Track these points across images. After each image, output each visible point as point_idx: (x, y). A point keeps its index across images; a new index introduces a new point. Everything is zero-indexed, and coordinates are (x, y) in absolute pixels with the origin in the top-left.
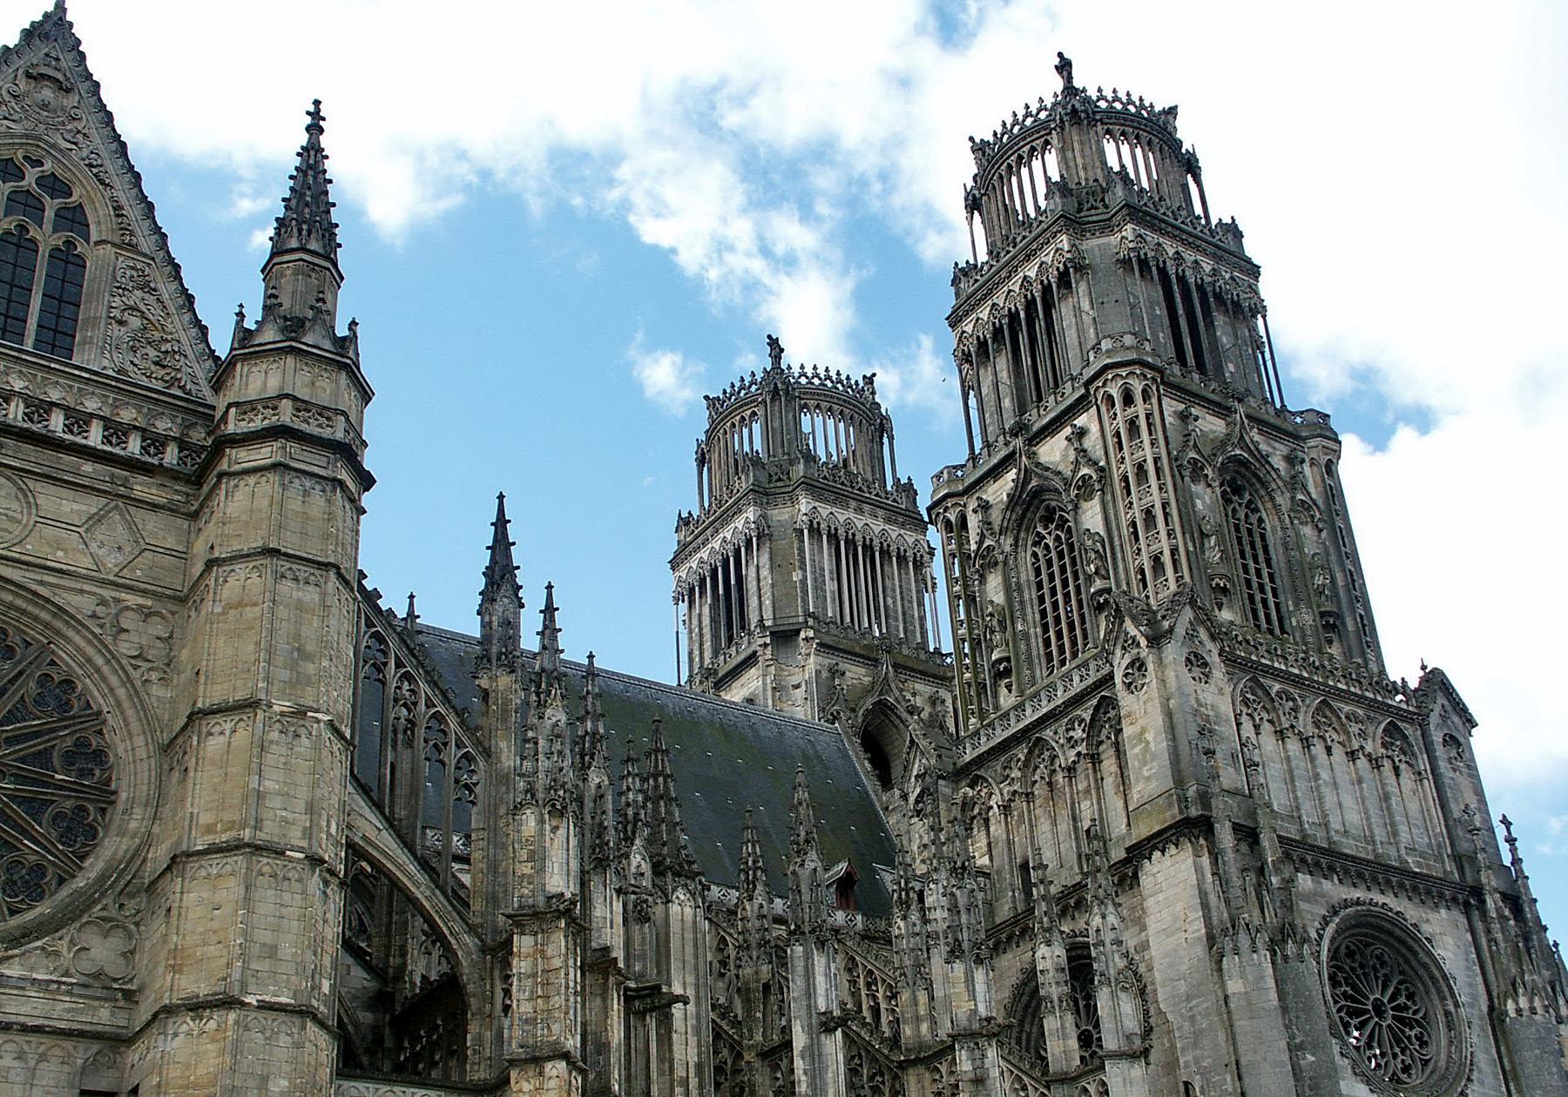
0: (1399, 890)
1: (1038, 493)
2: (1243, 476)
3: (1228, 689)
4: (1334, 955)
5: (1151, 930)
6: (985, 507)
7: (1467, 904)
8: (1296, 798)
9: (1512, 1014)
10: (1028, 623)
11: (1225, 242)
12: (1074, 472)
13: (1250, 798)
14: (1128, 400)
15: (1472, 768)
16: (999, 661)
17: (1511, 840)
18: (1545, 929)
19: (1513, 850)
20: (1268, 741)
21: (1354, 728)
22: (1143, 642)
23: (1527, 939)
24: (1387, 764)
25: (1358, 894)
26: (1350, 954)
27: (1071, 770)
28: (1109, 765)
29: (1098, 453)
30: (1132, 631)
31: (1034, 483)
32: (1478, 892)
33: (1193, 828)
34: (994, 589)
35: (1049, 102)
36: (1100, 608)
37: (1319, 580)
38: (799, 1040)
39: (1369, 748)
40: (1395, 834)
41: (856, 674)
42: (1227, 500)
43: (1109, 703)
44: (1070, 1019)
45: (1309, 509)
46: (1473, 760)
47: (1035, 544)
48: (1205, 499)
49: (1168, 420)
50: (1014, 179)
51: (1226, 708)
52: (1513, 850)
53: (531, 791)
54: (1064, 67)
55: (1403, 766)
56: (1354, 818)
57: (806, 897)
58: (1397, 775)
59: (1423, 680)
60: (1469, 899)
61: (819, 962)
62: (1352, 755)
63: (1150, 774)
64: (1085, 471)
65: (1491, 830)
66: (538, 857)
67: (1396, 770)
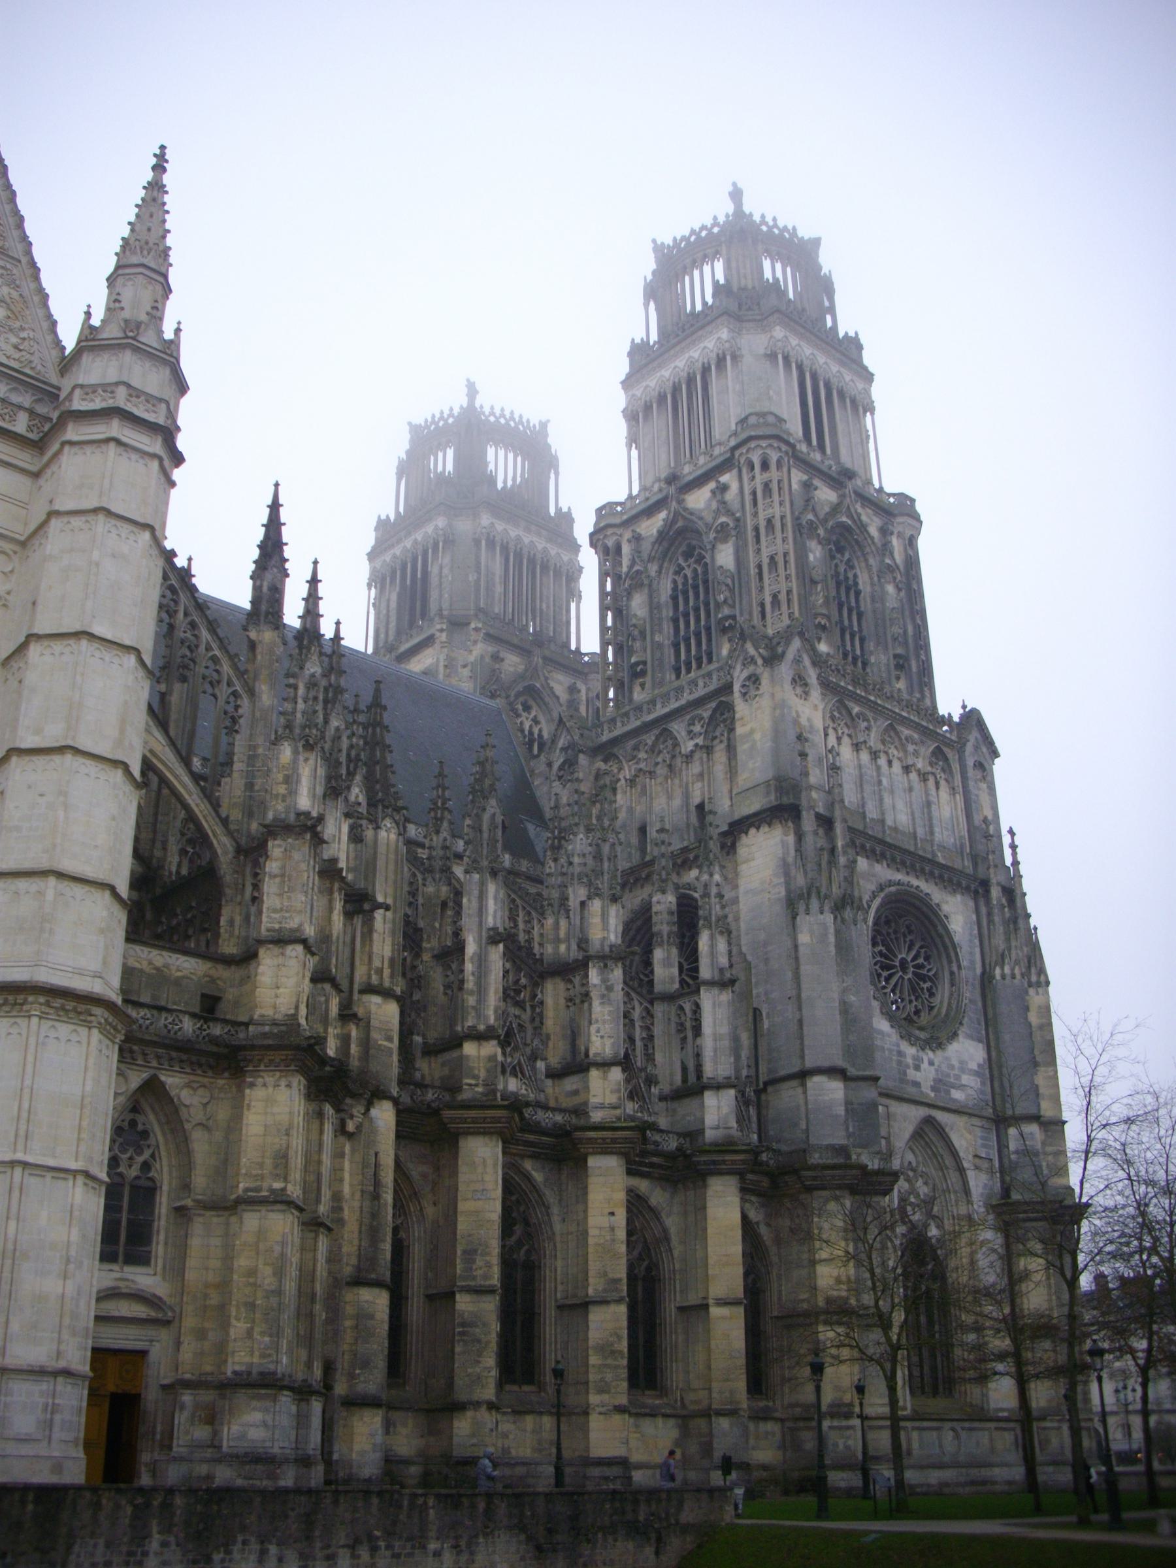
0: (930, 876)
1: (681, 532)
3: (821, 707)
4: (876, 923)
5: (742, 889)
6: (637, 539)
7: (976, 892)
9: (998, 977)
10: (664, 636)
11: (849, 351)
12: (715, 519)
13: (832, 793)
14: (765, 466)
16: (637, 664)
17: (1013, 847)
18: (1029, 916)
19: (1014, 854)
21: (911, 748)
22: (760, 661)
23: (1015, 922)
25: (899, 876)
26: (888, 922)
27: (689, 757)
28: (720, 755)
29: (736, 506)
30: (751, 651)
31: (680, 524)
32: (985, 884)
33: (783, 809)
34: (638, 605)
36: (724, 630)
37: (896, 630)
38: (471, 948)
39: (919, 765)
40: (932, 833)
41: (512, 663)
42: (833, 557)
43: (729, 707)
44: (674, 951)
45: (892, 571)
47: (677, 573)
48: (815, 553)
49: (795, 486)
50: (687, 278)
51: (819, 724)
52: (1014, 854)
53: (289, 726)
55: (943, 783)
56: (903, 819)
57: (485, 835)
58: (938, 788)
59: (962, 717)
60: (978, 889)
61: (491, 888)
62: (907, 769)
63: (755, 767)
64: (723, 519)
65: (1000, 837)
66: (291, 780)
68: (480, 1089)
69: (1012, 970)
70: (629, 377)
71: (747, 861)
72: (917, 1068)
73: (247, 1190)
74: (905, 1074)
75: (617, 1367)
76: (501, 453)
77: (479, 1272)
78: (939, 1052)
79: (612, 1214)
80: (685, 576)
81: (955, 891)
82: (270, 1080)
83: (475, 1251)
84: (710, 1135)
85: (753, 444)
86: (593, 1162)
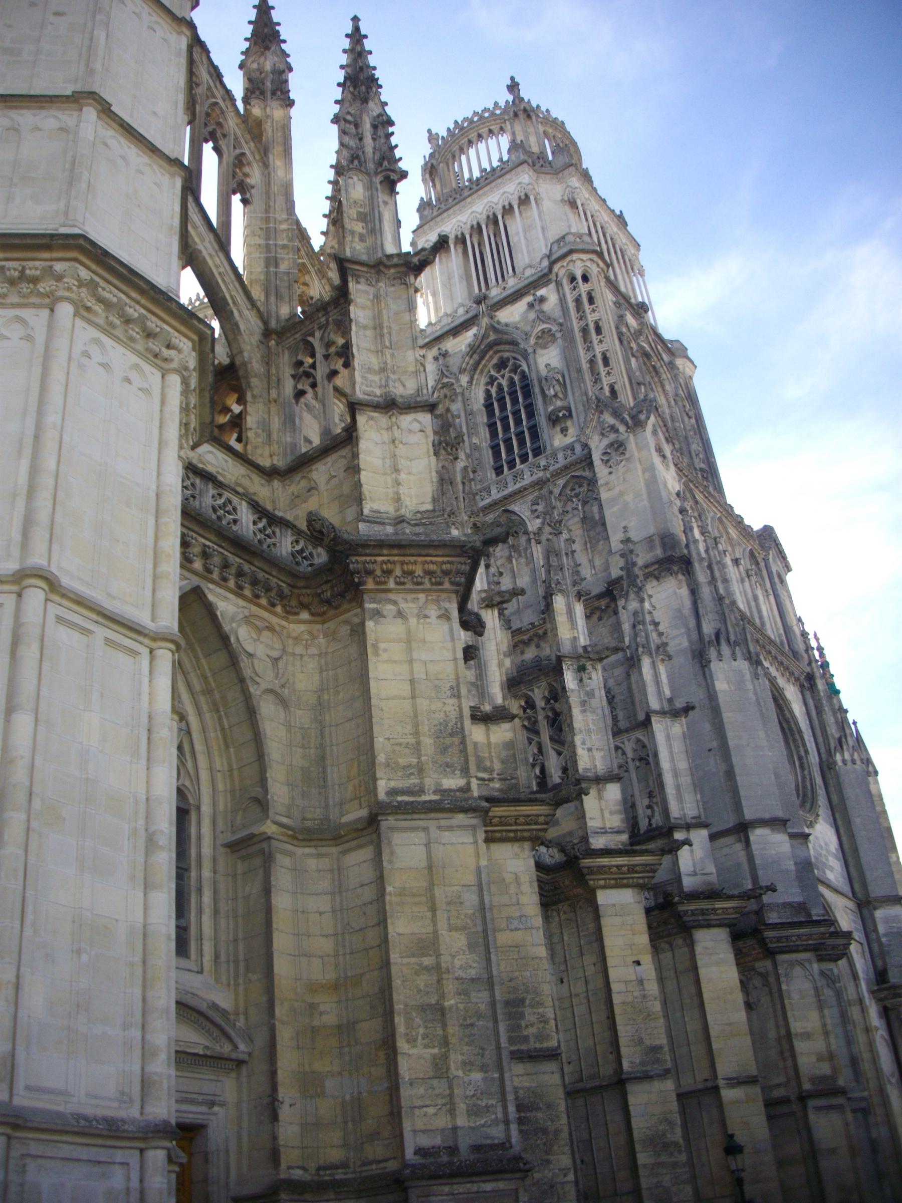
9: (840, 763)
14: (585, 278)
18: (846, 711)
35: (502, 104)
54: (513, 87)
68: (497, 785)
69: (852, 756)
70: (419, 227)
73: (393, 792)
75: (675, 1165)
77: (532, 1031)
79: (638, 963)
80: (500, 385)
82: (409, 605)
83: (523, 1001)
84: (688, 883)
85: (575, 256)
86: (604, 897)
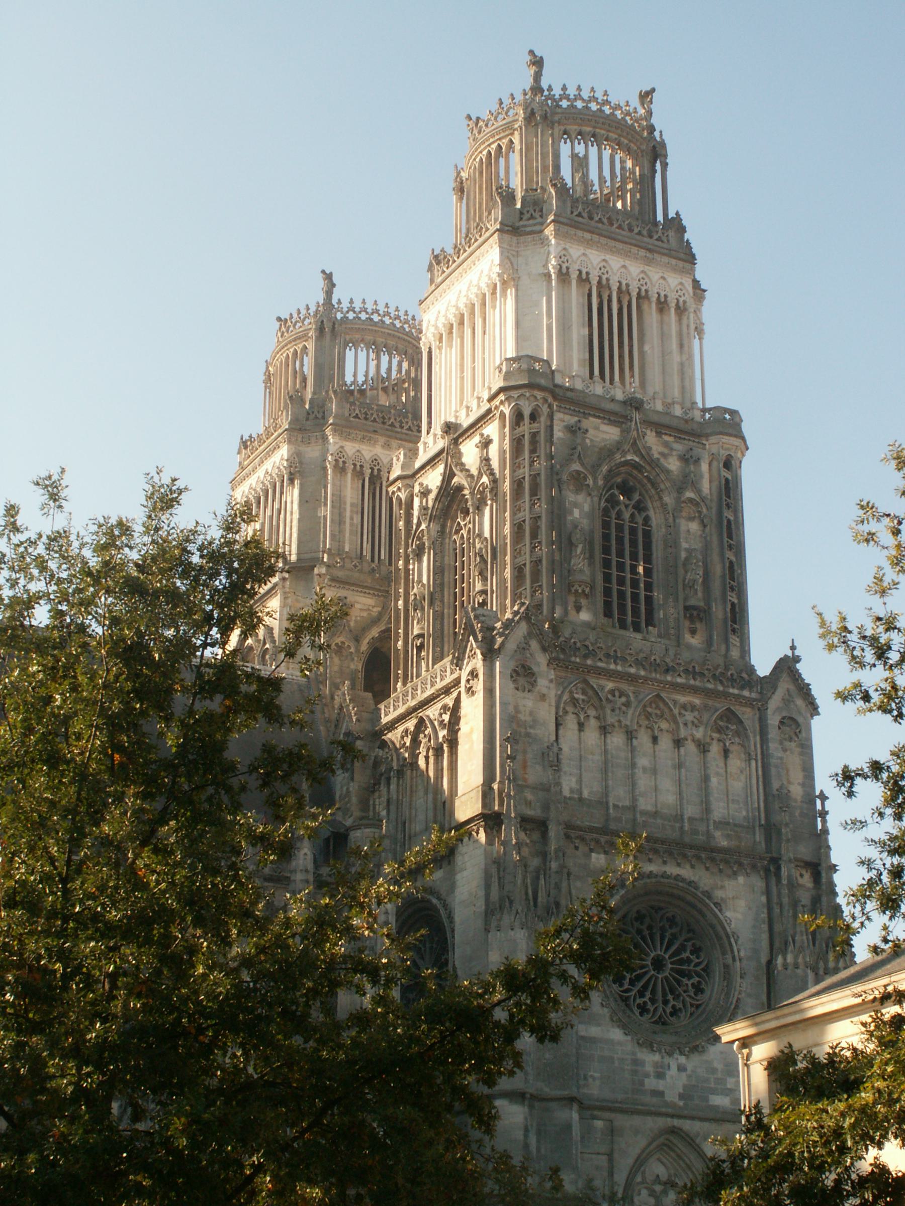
2: (635, 478)
6: (425, 493)
7: (767, 871)
8: (607, 787)
9: (780, 967)
15: (806, 749)
20: (592, 736)
21: (689, 716)
24: (715, 749)
26: (640, 917)
32: (776, 862)
40: (708, 810)
46: (809, 739)
48: (581, 509)
49: (558, 433)
50: (502, 161)
54: (538, 63)
55: (733, 748)
60: (771, 867)
62: (678, 743)
67: (726, 753)
71: (462, 870)
72: (660, 1075)
74: (642, 1083)
76: (362, 355)
78: (696, 1059)
81: (735, 873)
